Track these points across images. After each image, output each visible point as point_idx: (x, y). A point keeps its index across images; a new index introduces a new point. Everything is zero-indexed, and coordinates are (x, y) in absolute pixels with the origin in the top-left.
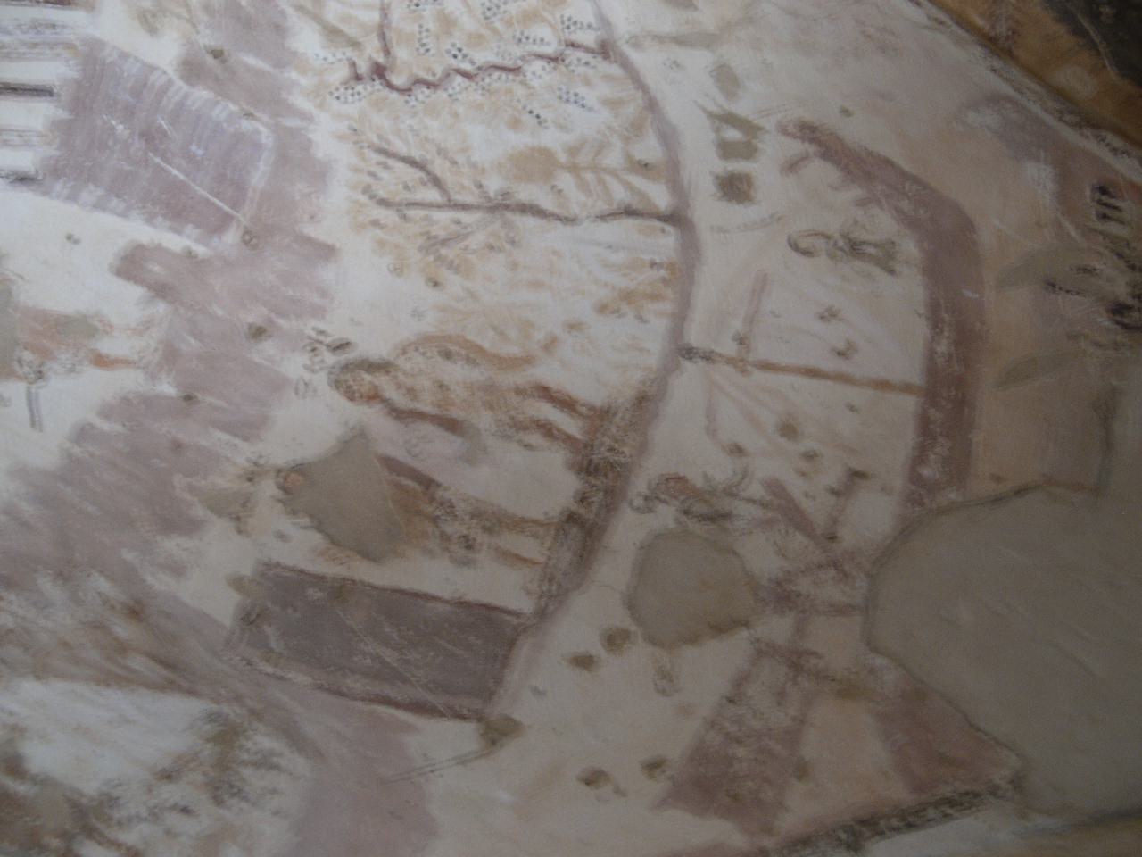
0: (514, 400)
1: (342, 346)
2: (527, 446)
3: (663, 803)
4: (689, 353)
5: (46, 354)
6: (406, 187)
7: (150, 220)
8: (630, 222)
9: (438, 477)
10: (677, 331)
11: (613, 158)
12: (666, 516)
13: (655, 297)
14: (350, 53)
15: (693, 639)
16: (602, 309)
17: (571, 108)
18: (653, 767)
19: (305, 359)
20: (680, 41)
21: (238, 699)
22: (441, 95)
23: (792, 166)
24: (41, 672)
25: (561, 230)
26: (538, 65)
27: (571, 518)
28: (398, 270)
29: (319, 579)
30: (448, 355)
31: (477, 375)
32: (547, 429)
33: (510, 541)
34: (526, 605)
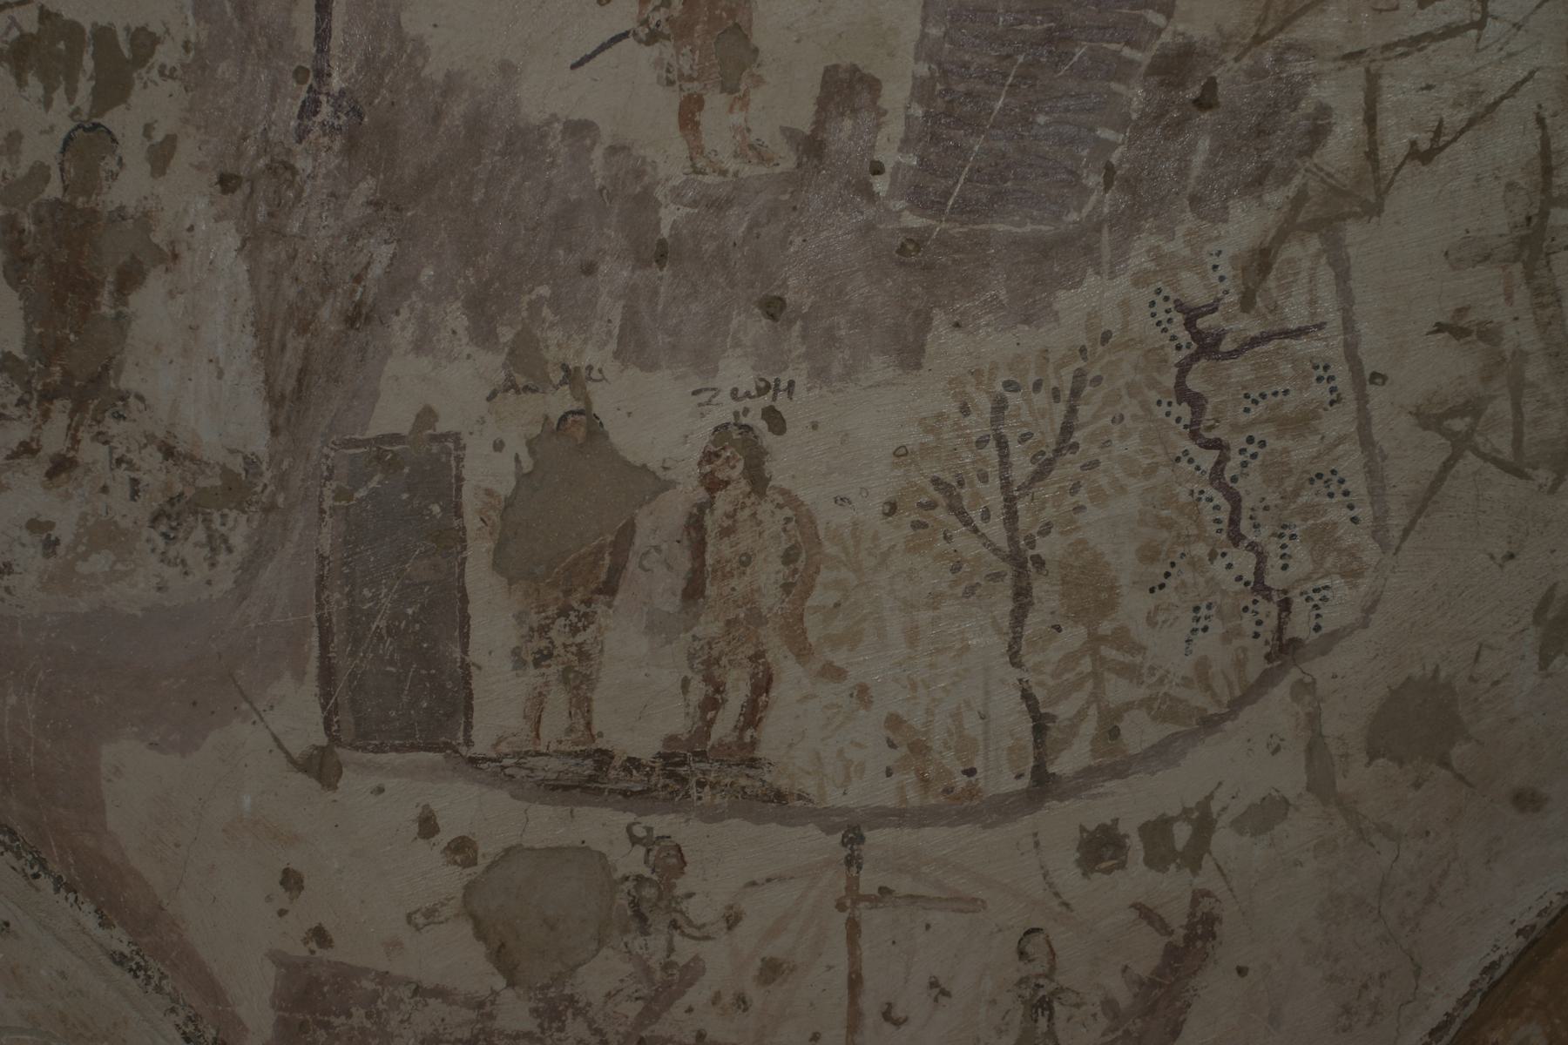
1: (775, 421)
2: (685, 684)
3: (278, 958)
4: (853, 837)
5: (682, 31)
7: (922, 90)
11: (1118, 690)
12: (631, 861)
13: (925, 782)
14: (1233, 298)
15: (481, 935)
16: (894, 722)
18: (320, 936)
19: (747, 382)
20: (1315, 748)
21: (282, 481)
23: (1146, 913)
24: (251, 243)
25: (999, 645)
26: (1244, 562)
27: (603, 758)
28: (901, 454)
30: (789, 558)
31: (771, 601)
32: (712, 703)
33: (558, 699)
34: (482, 745)
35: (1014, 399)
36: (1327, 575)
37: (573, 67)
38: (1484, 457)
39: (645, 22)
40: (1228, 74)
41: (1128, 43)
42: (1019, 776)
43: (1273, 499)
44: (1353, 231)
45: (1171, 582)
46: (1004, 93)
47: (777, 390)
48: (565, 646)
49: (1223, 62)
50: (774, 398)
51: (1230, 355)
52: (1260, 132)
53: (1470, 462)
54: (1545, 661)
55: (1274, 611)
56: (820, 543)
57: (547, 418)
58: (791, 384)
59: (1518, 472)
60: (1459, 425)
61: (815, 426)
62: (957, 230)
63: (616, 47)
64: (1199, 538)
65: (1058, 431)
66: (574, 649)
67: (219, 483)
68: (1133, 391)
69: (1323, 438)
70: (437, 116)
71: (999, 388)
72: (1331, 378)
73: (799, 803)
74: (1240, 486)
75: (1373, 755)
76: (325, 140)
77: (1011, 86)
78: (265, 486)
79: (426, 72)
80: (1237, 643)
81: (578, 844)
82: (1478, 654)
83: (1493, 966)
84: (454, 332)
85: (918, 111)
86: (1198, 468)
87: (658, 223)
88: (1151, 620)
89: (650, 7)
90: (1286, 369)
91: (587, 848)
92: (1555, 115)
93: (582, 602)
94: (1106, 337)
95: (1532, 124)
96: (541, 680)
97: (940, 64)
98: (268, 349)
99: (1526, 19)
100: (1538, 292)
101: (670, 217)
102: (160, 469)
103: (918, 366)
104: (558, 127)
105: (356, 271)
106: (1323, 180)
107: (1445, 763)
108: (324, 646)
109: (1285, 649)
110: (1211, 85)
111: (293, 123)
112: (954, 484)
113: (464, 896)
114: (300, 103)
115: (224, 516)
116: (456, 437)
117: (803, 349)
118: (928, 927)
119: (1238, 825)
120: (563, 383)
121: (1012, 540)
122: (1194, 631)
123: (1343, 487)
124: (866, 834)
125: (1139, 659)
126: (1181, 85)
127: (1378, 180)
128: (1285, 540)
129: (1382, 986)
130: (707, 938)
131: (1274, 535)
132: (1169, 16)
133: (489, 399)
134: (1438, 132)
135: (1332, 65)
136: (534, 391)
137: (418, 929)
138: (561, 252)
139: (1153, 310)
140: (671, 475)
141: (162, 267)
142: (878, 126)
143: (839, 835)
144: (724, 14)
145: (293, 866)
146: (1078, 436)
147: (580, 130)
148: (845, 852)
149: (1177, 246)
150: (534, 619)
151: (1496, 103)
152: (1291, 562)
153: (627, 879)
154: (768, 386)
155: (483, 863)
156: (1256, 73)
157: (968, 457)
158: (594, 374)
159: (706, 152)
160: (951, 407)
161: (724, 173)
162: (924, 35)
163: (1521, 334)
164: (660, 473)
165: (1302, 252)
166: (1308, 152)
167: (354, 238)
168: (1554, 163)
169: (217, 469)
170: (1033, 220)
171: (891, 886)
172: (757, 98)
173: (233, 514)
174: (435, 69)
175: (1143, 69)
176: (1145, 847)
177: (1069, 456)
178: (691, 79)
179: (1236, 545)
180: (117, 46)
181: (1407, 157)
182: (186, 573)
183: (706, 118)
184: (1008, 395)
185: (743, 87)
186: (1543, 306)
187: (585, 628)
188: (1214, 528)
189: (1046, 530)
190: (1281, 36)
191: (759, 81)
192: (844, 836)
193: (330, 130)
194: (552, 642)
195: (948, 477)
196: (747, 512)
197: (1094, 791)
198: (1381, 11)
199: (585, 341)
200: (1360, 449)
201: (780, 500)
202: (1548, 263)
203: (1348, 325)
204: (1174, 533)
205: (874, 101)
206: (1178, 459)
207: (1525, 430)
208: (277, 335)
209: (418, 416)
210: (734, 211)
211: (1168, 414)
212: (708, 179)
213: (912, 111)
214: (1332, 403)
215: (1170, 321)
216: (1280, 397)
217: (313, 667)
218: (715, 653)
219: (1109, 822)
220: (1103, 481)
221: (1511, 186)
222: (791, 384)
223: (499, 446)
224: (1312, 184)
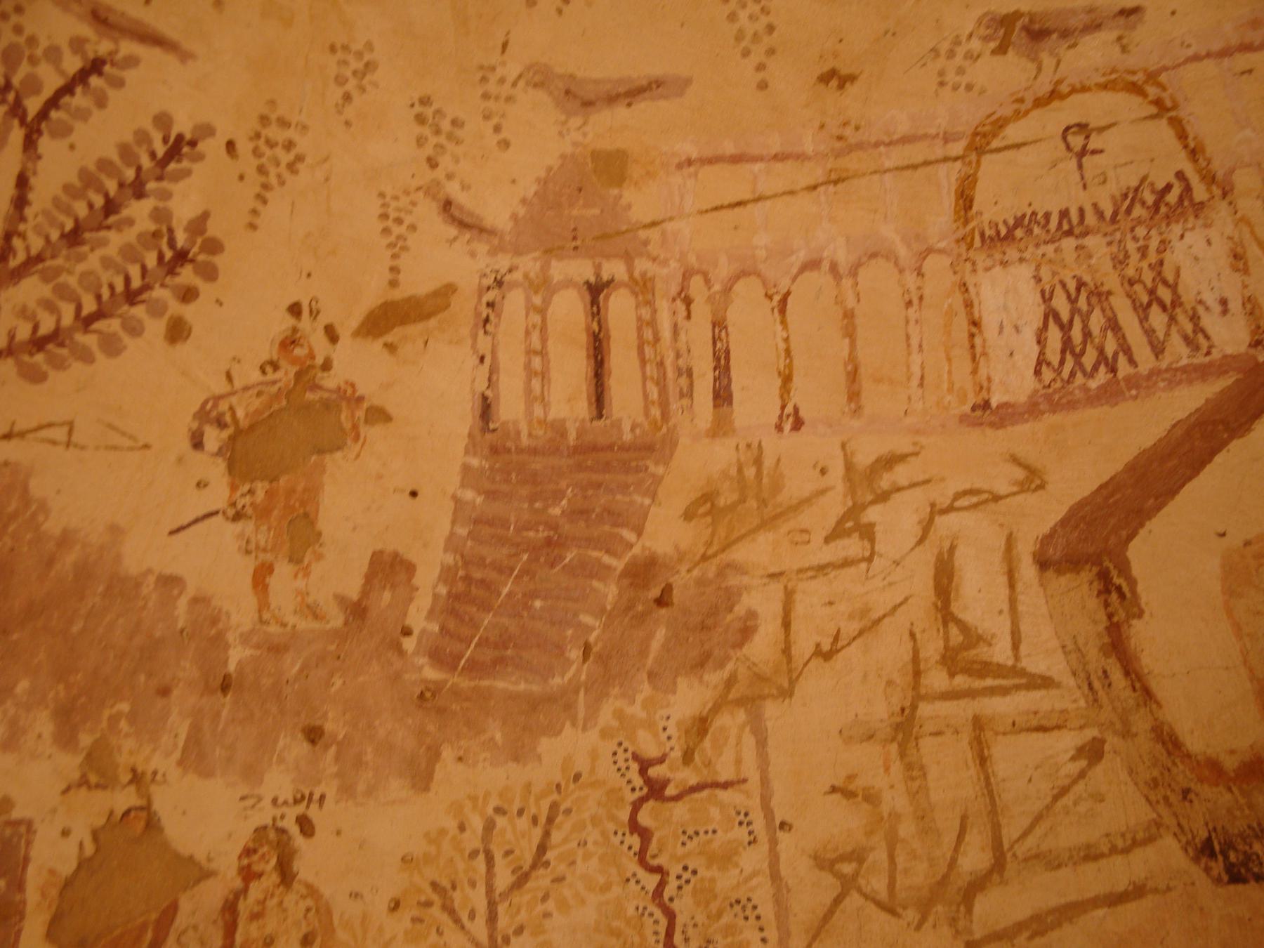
1: (306, 825)
5: (263, 513)
7: (447, 575)
14: (677, 754)
19: (286, 794)
22: (632, 866)
28: (406, 860)
29: (20, 886)
35: (501, 821)
37: (172, 533)
38: (866, 896)
39: (234, 504)
40: (682, 581)
41: (608, 551)
43: (701, 918)
44: (771, 709)
46: (510, 583)
50: (308, 806)
52: (704, 627)
53: (853, 900)
56: (334, 931)
58: (322, 798)
59: (892, 911)
60: (847, 868)
62: (465, 683)
65: (535, 849)
68: (595, 821)
69: (742, 871)
70: (50, 562)
71: (490, 811)
72: (749, 824)
74: (676, 906)
77: (517, 576)
79: (46, 526)
85: (443, 590)
86: (643, 888)
89: (239, 493)
90: (715, 812)
92: (924, 631)
94: (577, 777)
95: (906, 637)
97: (462, 556)
99: (903, 558)
100: (909, 767)
101: (236, 656)
103: (427, 789)
104: (151, 579)
106: (749, 668)
110: (668, 589)
112: (449, 886)
116: (29, 824)
117: (334, 769)
121: (492, 937)
123: (756, 912)
126: (646, 586)
127: (790, 671)
132: (640, 535)
134: (836, 638)
140: (214, 866)
142: (411, 599)
144: (297, 505)
146: (550, 855)
147: (170, 582)
149: (636, 710)
151: (879, 620)
154: (303, 797)
156: (700, 582)
157: (461, 866)
158: (159, 777)
159: (272, 607)
160: (451, 824)
161: (284, 625)
162: (452, 534)
163: (895, 799)
165: (731, 721)
166: (739, 645)
168: (922, 667)
170: (526, 681)
172: (317, 569)
174: (53, 526)
175: (618, 572)
178: (265, 550)
181: (813, 655)
183: (274, 582)
185: (306, 561)
186: (913, 779)
189: (520, 931)
190: (723, 556)
195: (445, 883)
196: (275, 901)
199: (154, 750)
200: (770, 883)
202: (917, 745)
203: (765, 781)
205: (409, 580)
206: (628, 880)
210: (288, 658)
212: (273, 629)
213: (437, 590)
214: (750, 843)
215: (627, 768)
220: (567, 892)
221: (890, 683)
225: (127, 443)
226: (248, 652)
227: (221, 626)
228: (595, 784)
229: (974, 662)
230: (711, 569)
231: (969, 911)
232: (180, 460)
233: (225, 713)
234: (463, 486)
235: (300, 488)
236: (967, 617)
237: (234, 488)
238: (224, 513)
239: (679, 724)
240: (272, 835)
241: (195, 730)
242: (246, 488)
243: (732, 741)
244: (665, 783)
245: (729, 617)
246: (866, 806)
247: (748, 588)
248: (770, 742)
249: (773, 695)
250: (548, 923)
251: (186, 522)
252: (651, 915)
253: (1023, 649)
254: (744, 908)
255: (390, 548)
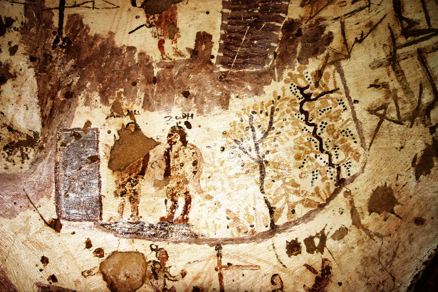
0: (183, 191)
1: (188, 125)
2: (166, 201)
4: (218, 247)
5: (158, 24)
6: (259, 126)
7: (223, 37)
8: (267, 211)
9: (145, 177)
10: (227, 241)
12: (152, 256)
13: (239, 230)
14: (313, 85)
15: (105, 278)
16: (228, 211)
17: (311, 176)
18: (53, 278)
20: (353, 211)
22: (303, 125)
23: (309, 267)
25: (258, 187)
26: (326, 157)
28: (224, 133)
30: (195, 164)
31: (190, 175)
32: (174, 207)
33: (128, 206)
36: (350, 158)
37: (130, 33)
41: (277, 21)
42: (267, 227)
43: (331, 139)
44: (344, 64)
45: (305, 165)
47: (188, 116)
48: (130, 190)
49: (302, 24)
50: (188, 119)
51: (315, 99)
53: (386, 123)
54: (417, 178)
55: (336, 170)
57: (123, 125)
58: (192, 115)
60: (381, 112)
61: (200, 127)
62: (235, 71)
63: (141, 28)
64: (311, 151)
66: (133, 191)
67: (26, 139)
68: (288, 111)
70: (92, 45)
71: (250, 113)
72: (343, 103)
73: (201, 238)
74: (322, 136)
75: (371, 212)
76: (60, 49)
78: (40, 141)
79: (89, 34)
80: (326, 181)
81: (135, 251)
82: (397, 178)
83: (417, 275)
84: (96, 101)
85: (222, 42)
86: (309, 132)
87: (153, 72)
88: (300, 177)
89: (150, 19)
90: (329, 101)
91: (138, 252)
93: (135, 177)
96: (123, 201)
97: (227, 30)
98: (42, 104)
100: (397, 72)
101: (156, 71)
102: (8, 134)
103: (227, 109)
104: (125, 48)
105: (68, 83)
106: (333, 51)
107: (393, 212)
108: (57, 190)
109: (340, 182)
110: (300, 30)
111: (52, 45)
112: (240, 140)
113: (100, 267)
114: (53, 40)
115: (27, 149)
116: (97, 129)
117: (195, 105)
118: (243, 275)
119: (333, 237)
120: (127, 115)
121: (259, 156)
122: (313, 179)
123: (351, 133)
124: (222, 246)
125: (298, 189)
126: (292, 31)
127: (348, 49)
128: (336, 150)
129: (384, 285)
130: (176, 280)
131: (333, 149)
132: (286, 14)
133: (106, 119)
134: (362, 34)
135: (331, 22)
136: (119, 117)
137: (85, 277)
138: (127, 80)
139: (291, 89)
140: (159, 141)
141: (11, 79)
142: (212, 46)
143: (214, 247)
145: (45, 256)
146: (274, 125)
147: (131, 49)
148: (217, 252)
149: (296, 72)
150: (121, 182)
152: (339, 156)
153: (150, 262)
154: (186, 116)
155: (106, 256)
156: (311, 26)
157: (243, 133)
158: (137, 113)
160: (238, 120)
161: (171, 59)
162: (222, 24)
164: (156, 140)
166: (328, 44)
167: (68, 74)
169: (25, 135)
170: (256, 68)
171: (231, 263)
172: (179, 40)
173: (30, 148)
174: (92, 33)
175: (281, 28)
176: (306, 246)
177: (272, 131)
178: (161, 36)
179: (322, 153)
180: (2, 20)
181: (355, 42)
182: (14, 164)
184: (253, 115)
185: (175, 38)
186: (399, 76)
187: (136, 185)
188: (315, 148)
189: (268, 152)
190: (316, 16)
191: (179, 36)
192: (216, 247)
193: (61, 47)
194: (126, 189)
197: (290, 230)
198: (342, 6)
199: (134, 104)
200: (354, 122)
201: (191, 147)
202: (398, 64)
203: (346, 88)
204: (304, 151)
205: (211, 40)
206: (303, 130)
207: (400, 111)
208: (45, 99)
209: (86, 123)
210: (173, 70)
211: (299, 117)
212: (168, 61)
214: (344, 110)
215: (296, 92)
216: (330, 110)
217: (53, 195)
218: (174, 192)
219: (295, 239)
221: (384, 45)
222: (192, 115)
223: (109, 132)
224: (330, 52)
225: (111, 6)
226: (160, 69)
227: (150, 61)
228: (286, 99)
229: (414, 31)
230: (314, 21)
231: (429, 117)
232: (129, 10)
233: (155, 90)
234: (223, 8)
235: (169, 15)
236: (409, 16)
237: (148, 17)
238: (146, 25)
239: (311, 74)
240: (177, 129)
241: (146, 96)
242: (151, 17)
243: (332, 76)
244: (311, 94)
245: (323, 36)
246: (384, 89)
247: (327, 25)
248: (346, 74)
249: (343, 58)
250: (277, 149)
251: (134, 30)
252: (313, 140)
253: (432, 22)
254: (346, 133)
255: (202, 31)
